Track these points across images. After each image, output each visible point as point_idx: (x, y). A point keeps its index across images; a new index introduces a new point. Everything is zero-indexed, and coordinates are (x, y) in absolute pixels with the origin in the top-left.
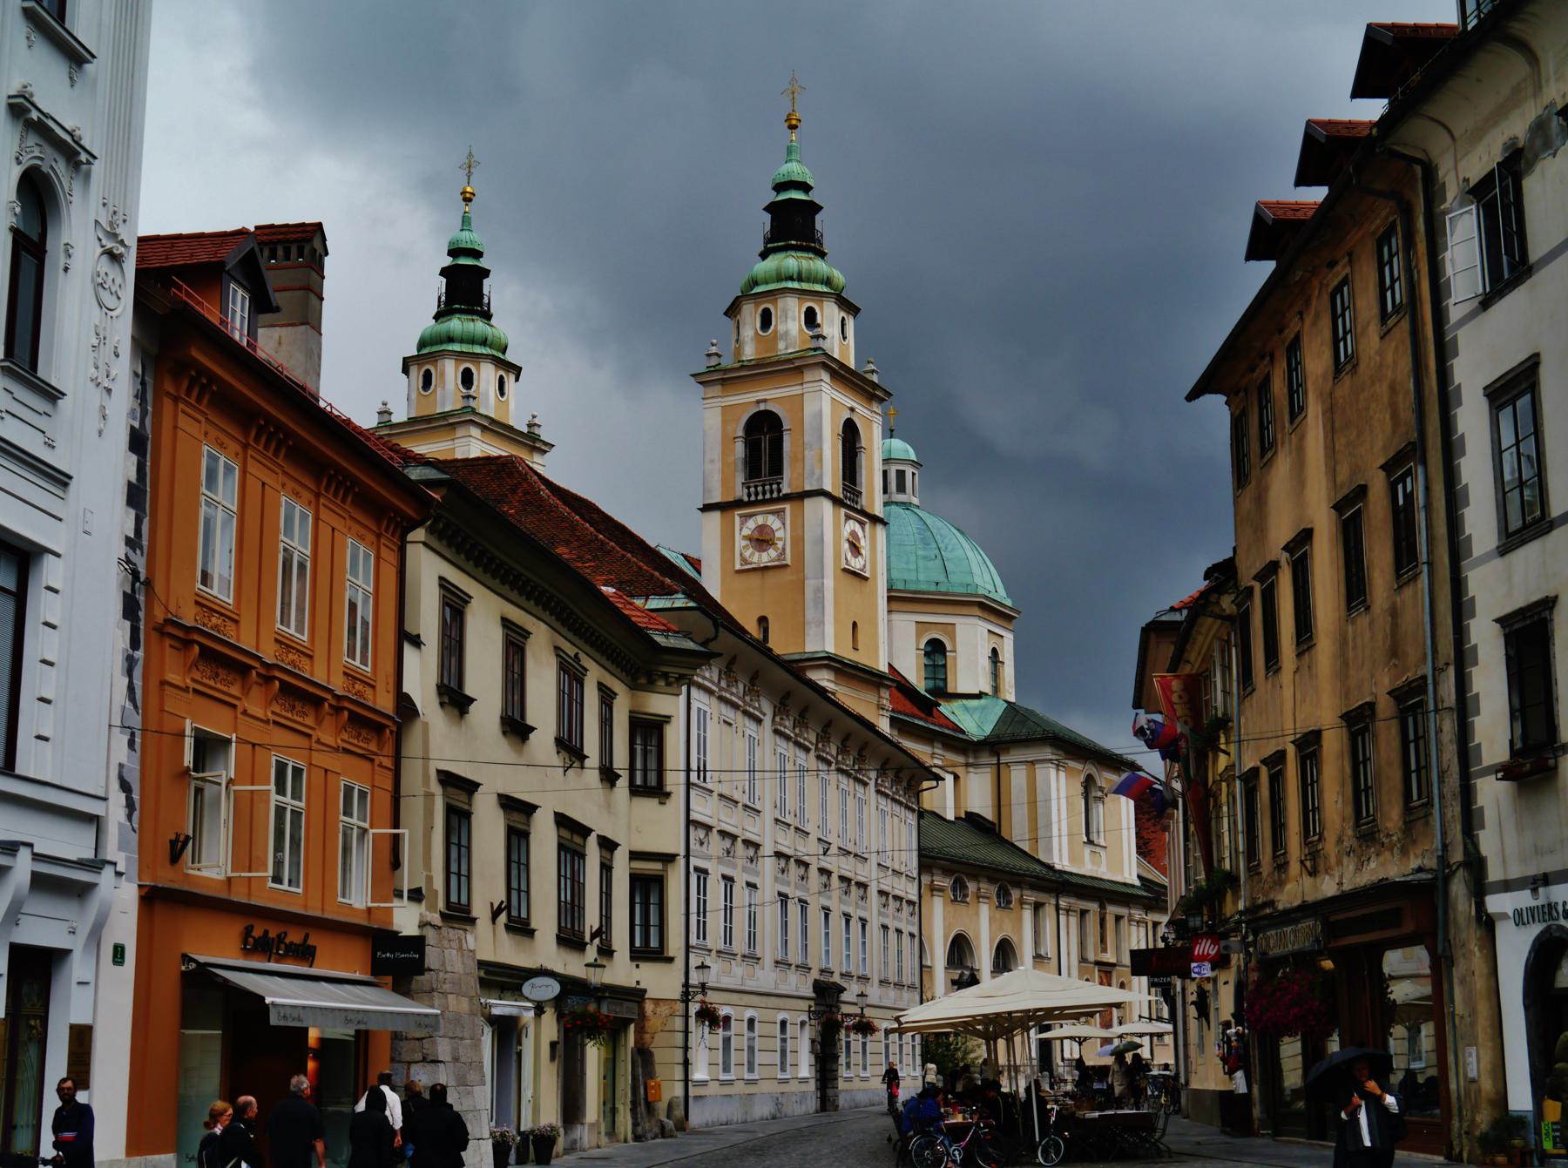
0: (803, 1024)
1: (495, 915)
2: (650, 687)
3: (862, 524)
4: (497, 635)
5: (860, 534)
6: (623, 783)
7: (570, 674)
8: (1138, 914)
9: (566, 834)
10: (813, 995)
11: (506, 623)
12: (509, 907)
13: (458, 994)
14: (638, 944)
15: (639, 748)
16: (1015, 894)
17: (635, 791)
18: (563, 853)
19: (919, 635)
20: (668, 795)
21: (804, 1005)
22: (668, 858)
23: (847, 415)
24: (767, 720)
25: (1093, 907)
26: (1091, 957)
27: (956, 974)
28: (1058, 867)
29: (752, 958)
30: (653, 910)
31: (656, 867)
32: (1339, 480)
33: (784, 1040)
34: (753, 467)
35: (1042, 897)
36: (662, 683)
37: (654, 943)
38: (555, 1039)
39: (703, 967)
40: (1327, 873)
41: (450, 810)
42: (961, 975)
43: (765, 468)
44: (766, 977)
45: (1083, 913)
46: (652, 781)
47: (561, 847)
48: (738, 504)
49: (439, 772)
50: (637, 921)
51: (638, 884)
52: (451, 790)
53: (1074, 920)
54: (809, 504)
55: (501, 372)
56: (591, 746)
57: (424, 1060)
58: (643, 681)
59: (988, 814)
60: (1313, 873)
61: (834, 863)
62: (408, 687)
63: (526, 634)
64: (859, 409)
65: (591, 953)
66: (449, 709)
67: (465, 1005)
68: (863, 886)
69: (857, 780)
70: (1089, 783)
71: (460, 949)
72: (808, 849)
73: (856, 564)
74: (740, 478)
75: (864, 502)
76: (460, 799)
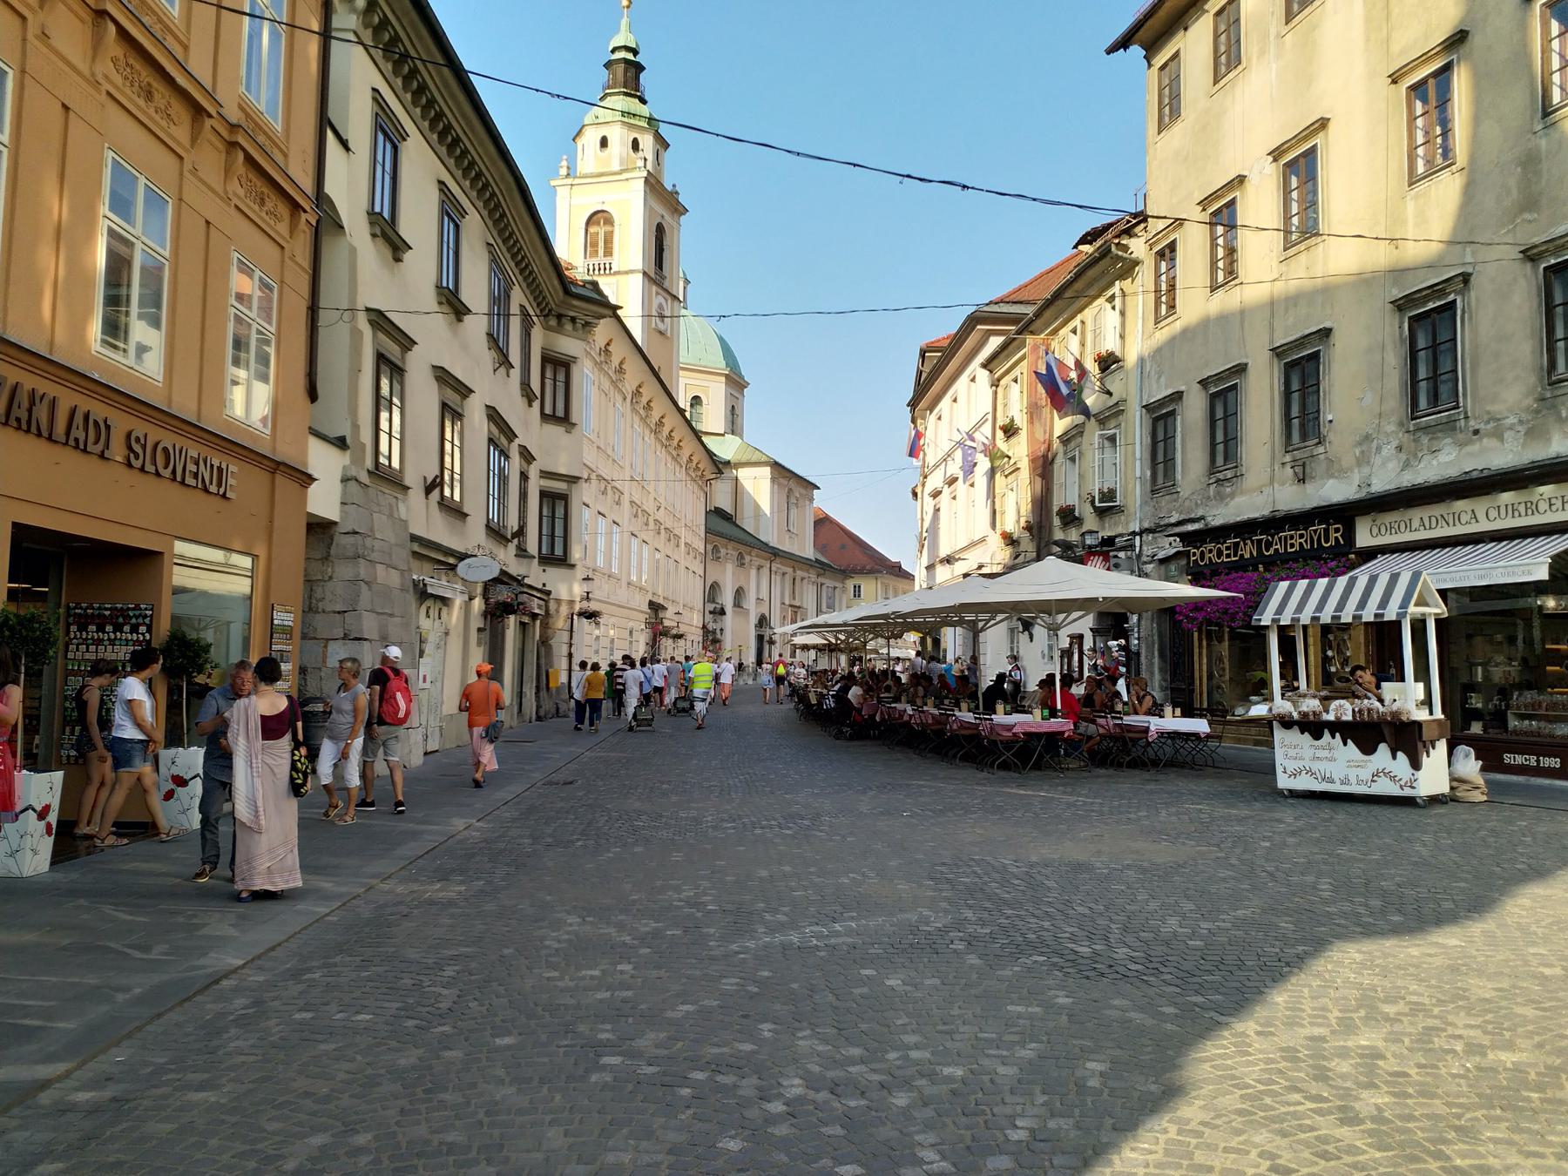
1: (429, 490)
2: (559, 329)
3: (666, 300)
5: (664, 304)
6: (537, 404)
8: (813, 577)
9: (495, 431)
12: (441, 484)
13: (388, 566)
14: (544, 551)
15: (548, 382)
16: (747, 558)
17: (545, 417)
18: (492, 448)
20: (575, 424)
21: (643, 617)
22: (573, 480)
23: (659, 220)
24: (629, 400)
25: (790, 570)
26: (787, 602)
27: (711, 607)
28: (771, 545)
31: (560, 486)
32: (1396, 48)
33: (631, 642)
35: (763, 562)
36: (569, 327)
37: (559, 551)
38: (482, 626)
39: (587, 579)
40: (1332, 476)
41: (381, 358)
42: (715, 608)
44: (622, 595)
45: (784, 574)
46: (560, 413)
47: (491, 441)
49: (368, 310)
50: (544, 532)
51: (545, 500)
52: (381, 336)
53: (778, 578)
56: (515, 356)
57: (345, 637)
58: (553, 322)
59: (729, 509)
60: (1302, 480)
61: (661, 515)
62: (330, 188)
64: (667, 217)
65: (512, 547)
66: (380, 241)
67: (394, 579)
68: (677, 537)
69: (676, 460)
70: (790, 490)
71: (391, 516)
72: (649, 506)
75: (666, 284)
76: (393, 350)
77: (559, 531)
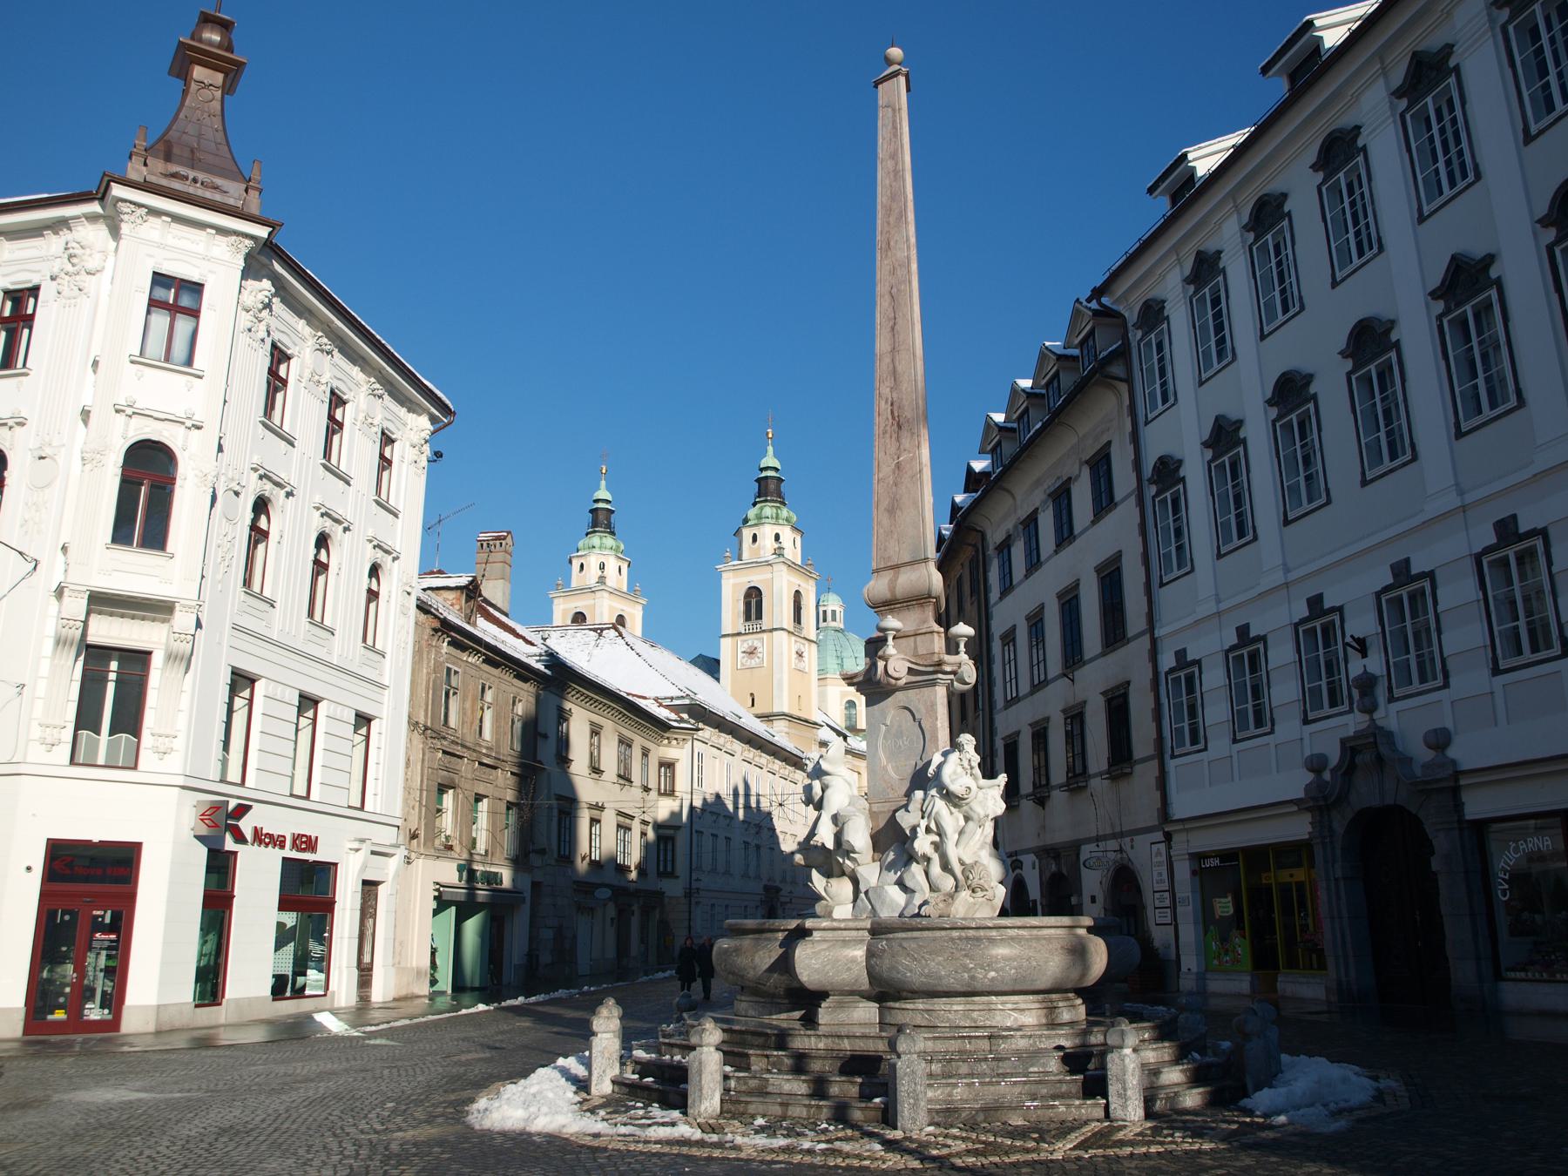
0: (757, 907)
4: (587, 729)
7: (625, 743)
10: (762, 892)
11: (592, 723)
14: (661, 869)
19: (842, 697)
29: (727, 873)
30: (670, 854)
31: (670, 832)
34: (748, 618)
36: (674, 742)
37: (669, 869)
39: (698, 880)
41: (561, 812)
43: (753, 616)
48: (739, 634)
54: (775, 633)
55: (620, 564)
63: (601, 727)
73: (801, 665)
74: (742, 619)
77: (669, 858)
